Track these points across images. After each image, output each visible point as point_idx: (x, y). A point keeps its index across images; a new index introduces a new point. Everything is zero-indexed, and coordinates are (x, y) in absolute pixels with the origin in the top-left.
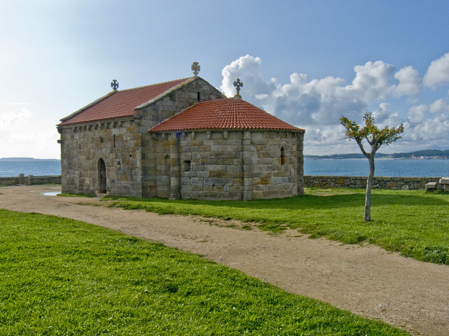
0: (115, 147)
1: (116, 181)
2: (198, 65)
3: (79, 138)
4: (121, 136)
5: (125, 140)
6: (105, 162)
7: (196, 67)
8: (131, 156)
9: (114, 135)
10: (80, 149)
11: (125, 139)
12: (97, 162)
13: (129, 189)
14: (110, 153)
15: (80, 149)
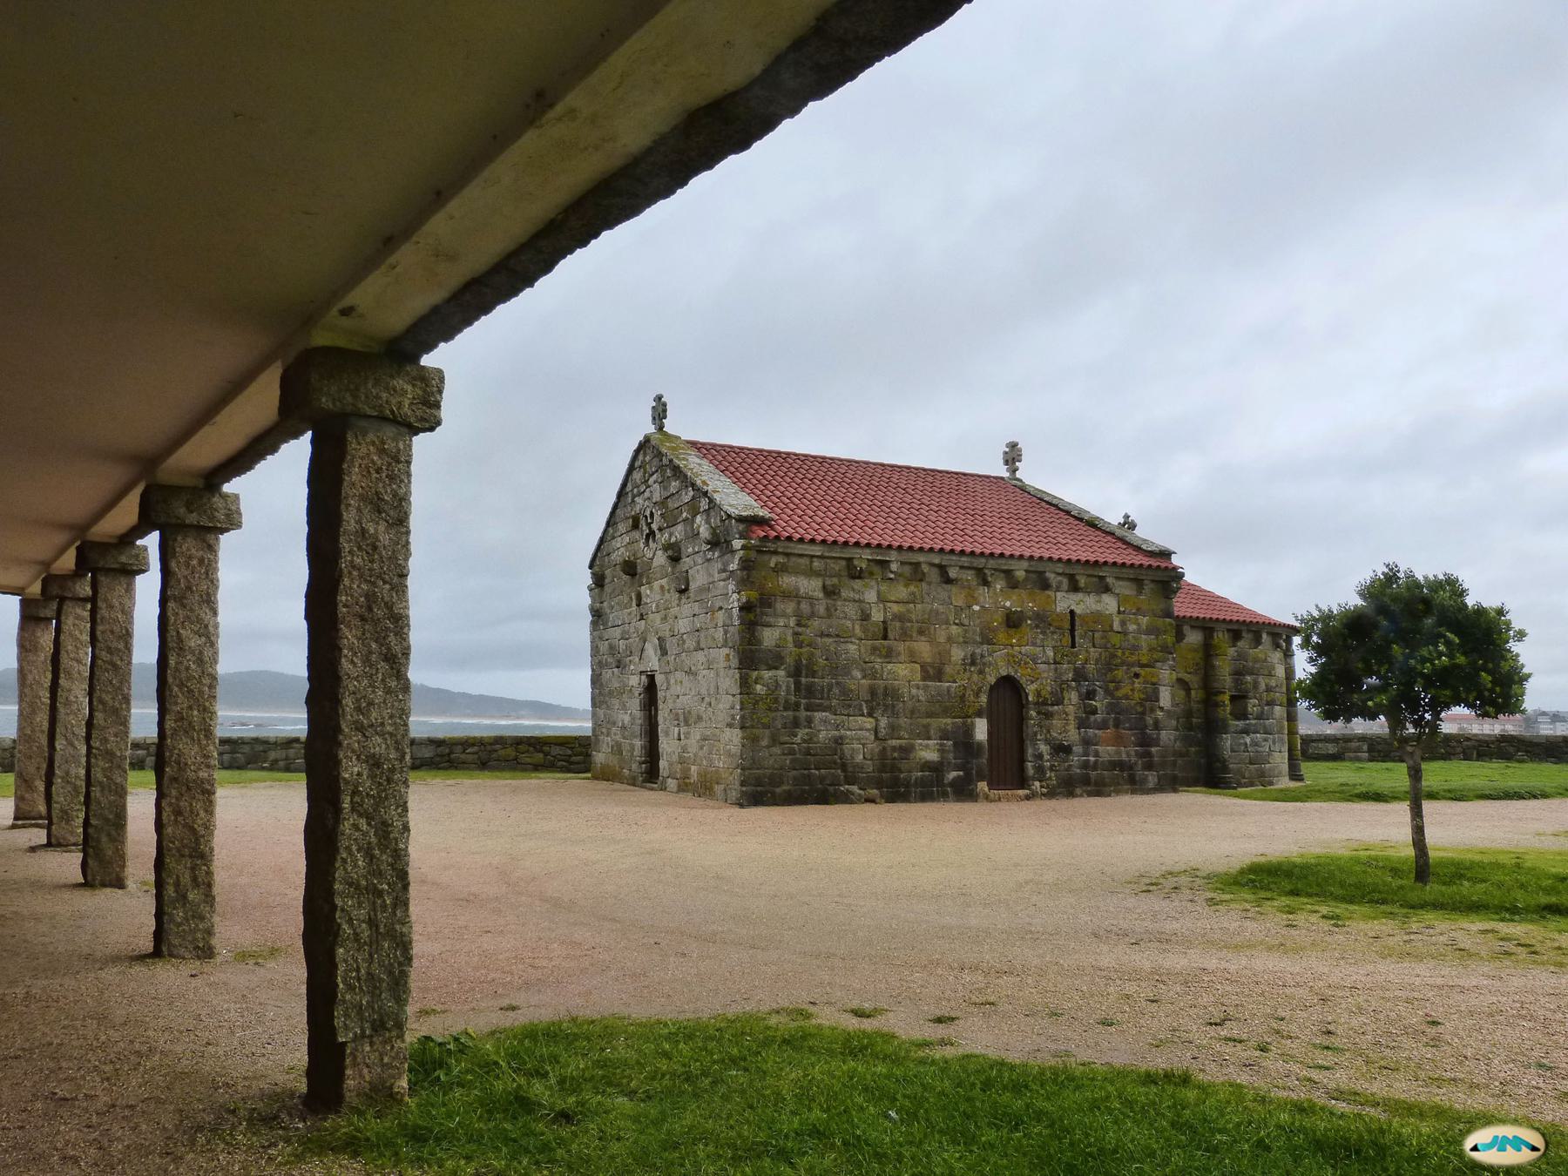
0: (1073, 646)
1: (1077, 749)
2: (1007, 450)
3: (882, 599)
4: (1098, 617)
5: (1120, 630)
6: (1031, 689)
7: (1012, 456)
8: (1137, 675)
9: (1072, 612)
10: (885, 637)
11: (1117, 626)
12: (986, 688)
13: (1131, 768)
14: (1055, 663)
15: (885, 637)
